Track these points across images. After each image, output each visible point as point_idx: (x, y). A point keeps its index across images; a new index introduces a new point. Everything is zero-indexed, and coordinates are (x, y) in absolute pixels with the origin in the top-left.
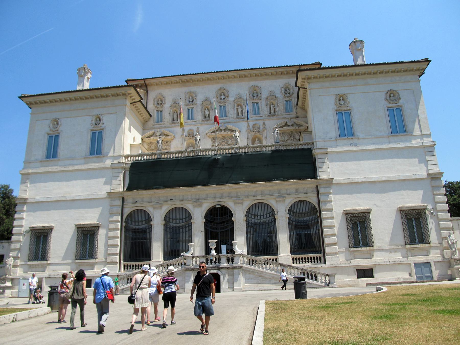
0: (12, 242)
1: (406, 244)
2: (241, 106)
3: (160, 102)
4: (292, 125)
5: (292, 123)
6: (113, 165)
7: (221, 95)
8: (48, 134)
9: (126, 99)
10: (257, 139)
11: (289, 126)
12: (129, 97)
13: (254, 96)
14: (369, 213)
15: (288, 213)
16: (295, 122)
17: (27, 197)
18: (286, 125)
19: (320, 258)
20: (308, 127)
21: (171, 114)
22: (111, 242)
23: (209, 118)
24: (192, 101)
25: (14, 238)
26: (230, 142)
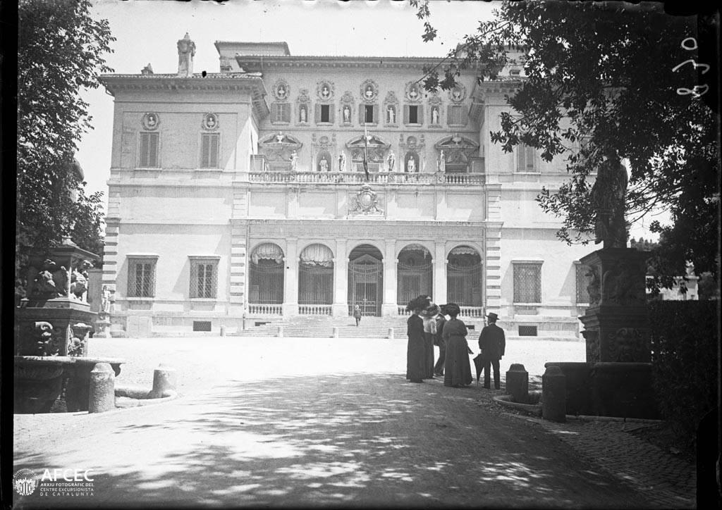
0: (103, 272)
1: (577, 302)
2: (394, 110)
3: (282, 92)
4: (459, 143)
5: (459, 139)
6: (234, 185)
7: (367, 90)
8: (141, 133)
9: (249, 94)
10: (412, 157)
11: (455, 143)
12: (252, 93)
13: (411, 97)
14: (541, 264)
15: (448, 259)
16: (463, 139)
17: (118, 216)
18: (451, 141)
19: (480, 311)
20: (479, 147)
21: (298, 113)
22: (235, 279)
23: (350, 121)
24: (328, 95)
25: (105, 267)
26: (376, 160)
